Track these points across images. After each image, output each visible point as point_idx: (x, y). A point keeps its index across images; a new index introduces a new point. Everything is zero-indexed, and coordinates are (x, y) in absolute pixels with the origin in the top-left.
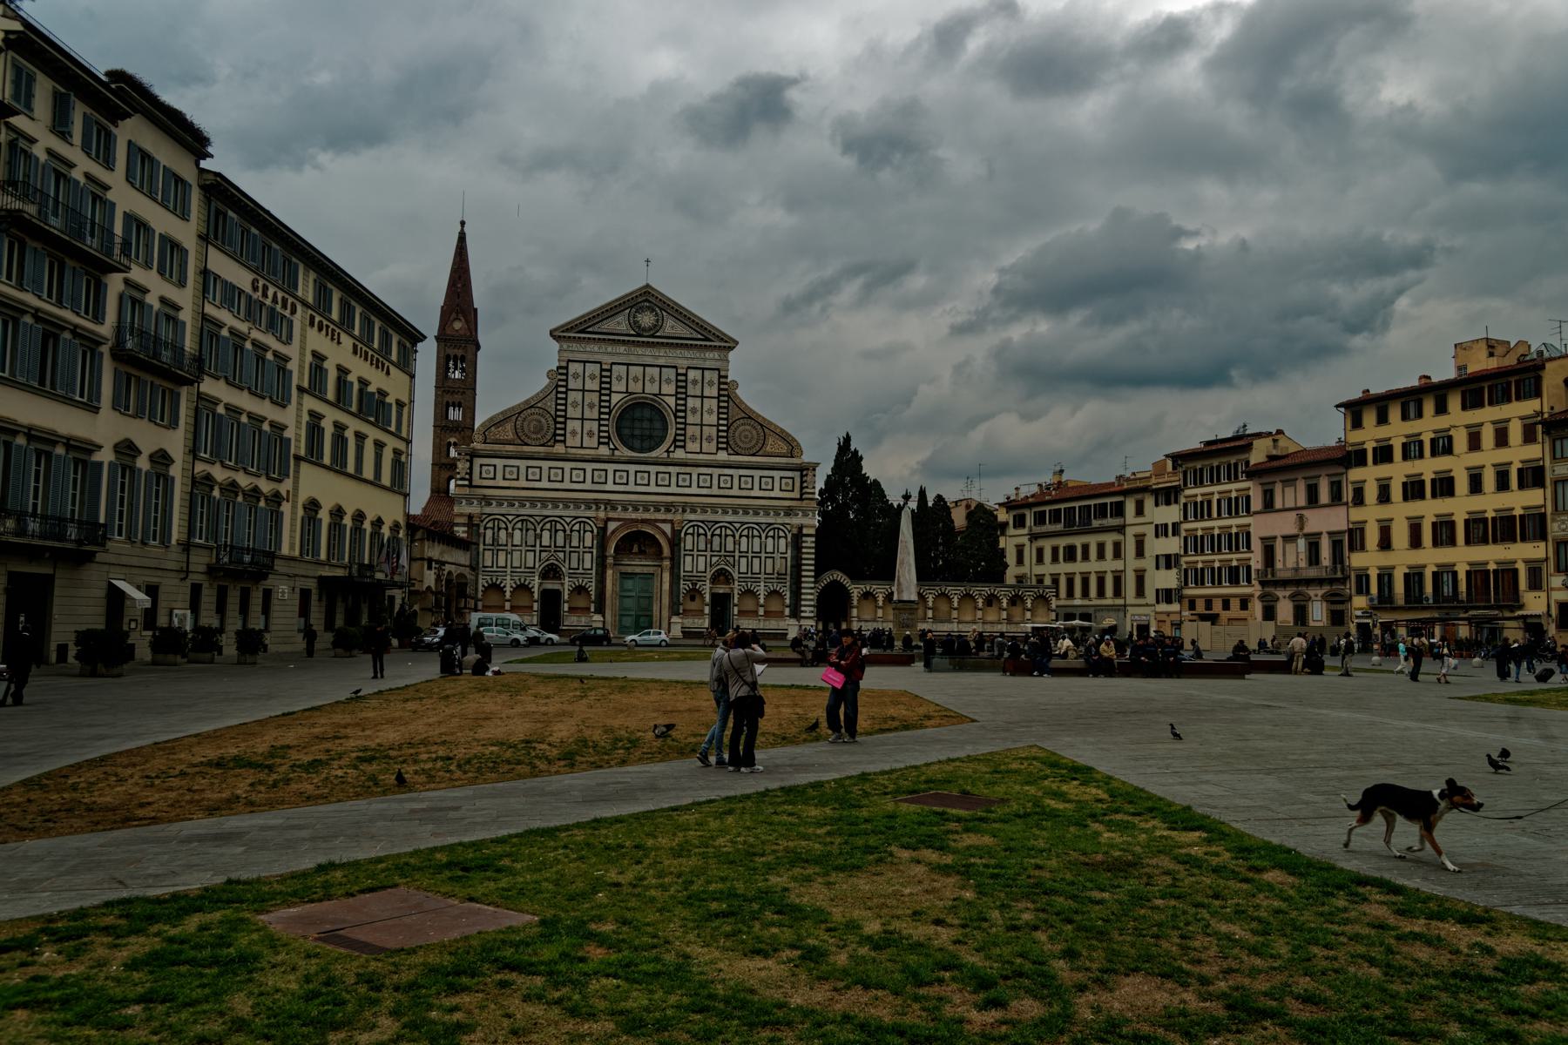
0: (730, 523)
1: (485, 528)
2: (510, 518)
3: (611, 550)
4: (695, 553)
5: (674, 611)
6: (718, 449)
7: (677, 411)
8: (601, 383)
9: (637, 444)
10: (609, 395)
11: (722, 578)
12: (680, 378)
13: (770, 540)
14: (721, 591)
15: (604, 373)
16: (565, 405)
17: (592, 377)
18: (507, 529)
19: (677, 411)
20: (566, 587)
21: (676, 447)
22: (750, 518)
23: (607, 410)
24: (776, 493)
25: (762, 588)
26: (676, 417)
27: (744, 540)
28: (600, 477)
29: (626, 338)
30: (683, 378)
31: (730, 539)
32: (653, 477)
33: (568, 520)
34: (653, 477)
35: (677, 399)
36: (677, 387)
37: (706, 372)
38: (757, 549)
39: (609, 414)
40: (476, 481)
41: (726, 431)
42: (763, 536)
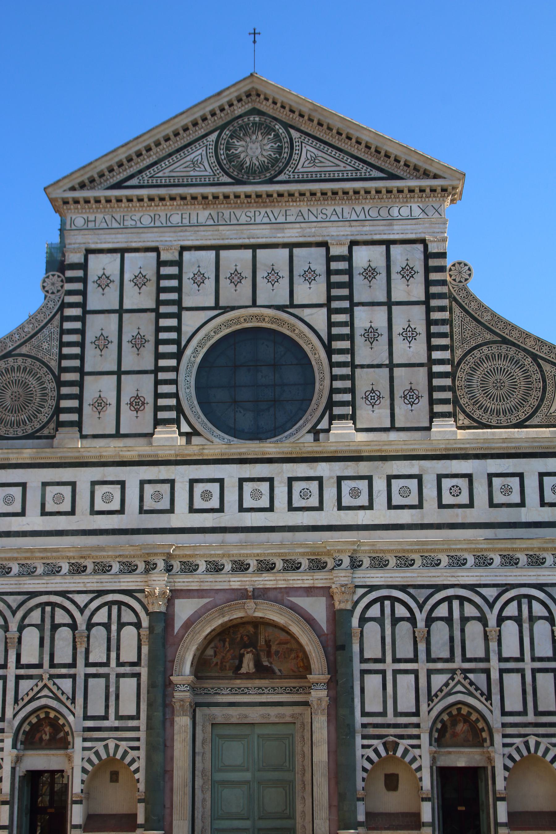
0: (472, 587)
4: (389, 666)
6: (433, 415)
7: (332, 337)
8: (160, 290)
10: (178, 316)
11: (461, 727)
12: (334, 266)
14: (461, 763)
15: (165, 271)
16: (82, 345)
20: (78, 763)
21: (332, 418)
23: (173, 348)
26: (330, 352)
28: (157, 496)
29: (209, 191)
30: (343, 265)
32: (281, 491)
33: (81, 600)
34: (281, 491)
35: (331, 312)
36: (330, 286)
37: (395, 250)
39: (178, 356)
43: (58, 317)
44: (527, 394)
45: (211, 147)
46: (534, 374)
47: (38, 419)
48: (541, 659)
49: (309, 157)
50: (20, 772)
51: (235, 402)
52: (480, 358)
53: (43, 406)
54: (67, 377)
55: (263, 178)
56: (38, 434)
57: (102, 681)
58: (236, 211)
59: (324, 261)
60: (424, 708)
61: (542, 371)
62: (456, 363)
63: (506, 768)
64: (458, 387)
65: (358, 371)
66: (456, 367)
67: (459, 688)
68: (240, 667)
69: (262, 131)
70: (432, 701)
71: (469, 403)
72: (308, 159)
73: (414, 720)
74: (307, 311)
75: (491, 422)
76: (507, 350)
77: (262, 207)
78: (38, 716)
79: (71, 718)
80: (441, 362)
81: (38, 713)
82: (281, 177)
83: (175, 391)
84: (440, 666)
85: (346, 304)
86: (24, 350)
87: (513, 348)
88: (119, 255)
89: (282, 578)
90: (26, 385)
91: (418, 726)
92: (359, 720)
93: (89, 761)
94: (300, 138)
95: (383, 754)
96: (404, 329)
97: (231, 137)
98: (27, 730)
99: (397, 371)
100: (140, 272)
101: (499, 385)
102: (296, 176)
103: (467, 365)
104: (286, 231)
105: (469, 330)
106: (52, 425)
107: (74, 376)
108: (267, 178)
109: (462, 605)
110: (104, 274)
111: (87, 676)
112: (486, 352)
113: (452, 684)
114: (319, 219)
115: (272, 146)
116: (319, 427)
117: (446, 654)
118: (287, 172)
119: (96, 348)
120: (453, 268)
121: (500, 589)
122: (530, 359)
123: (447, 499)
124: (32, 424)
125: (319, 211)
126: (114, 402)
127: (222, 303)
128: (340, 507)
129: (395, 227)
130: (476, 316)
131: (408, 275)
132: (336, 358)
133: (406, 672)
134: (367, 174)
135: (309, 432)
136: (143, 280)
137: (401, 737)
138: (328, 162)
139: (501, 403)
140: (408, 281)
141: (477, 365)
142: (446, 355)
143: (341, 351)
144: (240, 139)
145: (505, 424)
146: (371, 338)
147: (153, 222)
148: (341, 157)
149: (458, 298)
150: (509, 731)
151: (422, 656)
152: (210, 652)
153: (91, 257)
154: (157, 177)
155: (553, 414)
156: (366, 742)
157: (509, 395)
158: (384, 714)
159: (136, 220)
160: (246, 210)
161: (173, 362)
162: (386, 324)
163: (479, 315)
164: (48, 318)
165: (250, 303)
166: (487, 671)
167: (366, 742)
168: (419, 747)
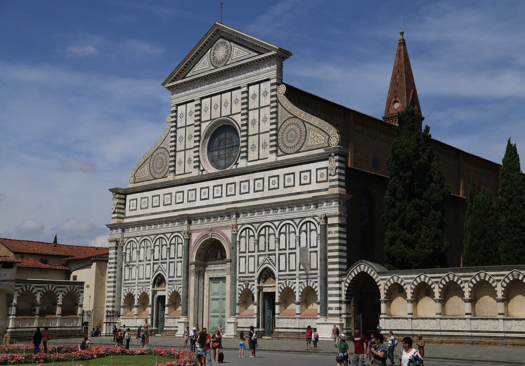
0: (271, 222)
1: (126, 249)
2: (138, 239)
3: (193, 259)
4: (247, 254)
5: (233, 314)
6: (271, 152)
7: (242, 125)
9: (222, 163)
10: (200, 125)
13: (303, 235)
16: (175, 141)
18: (136, 248)
19: (242, 125)
21: (242, 158)
22: (288, 214)
23: (197, 138)
24: (314, 186)
25: (297, 285)
27: (283, 237)
30: (245, 95)
31: (272, 238)
37: (262, 84)
38: (292, 245)
39: (199, 141)
40: (128, 213)
41: (276, 135)
42: (297, 231)
44: (300, 138)
48: (292, 249)
50: (156, 296)
55: (223, 64)
57: (173, 264)
60: (256, 270)
61: (305, 127)
63: (279, 292)
65: (249, 137)
67: (267, 262)
68: (217, 256)
70: (259, 267)
73: (253, 275)
74: (235, 116)
78: (160, 277)
79: (166, 278)
81: (160, 276)
82: (228, 63)
84: (262, 253)
86: (162, 146)
89: (219, 223)
90: (162, 159)
91: (254, 277)
92: (238, 275)
93: (170, 292)
95: (245, 288)
98: (158, 281)
101: (291, 136)
104: (229, 85)
106: (168, 172)
107: (172, 154)
109: (269, 229)
111: (170, 262)
112: (288, 122)
113: (265, 260)
117: (263, 249)
120: (279, 88)
121: (280, 222)
122: (302, 123)
123: (272, 187)
128: (240, 194)
129: (260, 76)
130: (286, 107)
133: (252, 256)
137: (250, 281)
141: (285, 129)
142: (274, 126)
143: (243, 131)
144: (216, 50)
149: (280, 101)
150: (281, 278)
151: (256, 250)
152: (209, 251)
156: (240, 283)
158: (245, 273)
161: (197, 144)
165: (220, 116)
166: (275, 254)
167: (240, 283)
168: (253, 285)
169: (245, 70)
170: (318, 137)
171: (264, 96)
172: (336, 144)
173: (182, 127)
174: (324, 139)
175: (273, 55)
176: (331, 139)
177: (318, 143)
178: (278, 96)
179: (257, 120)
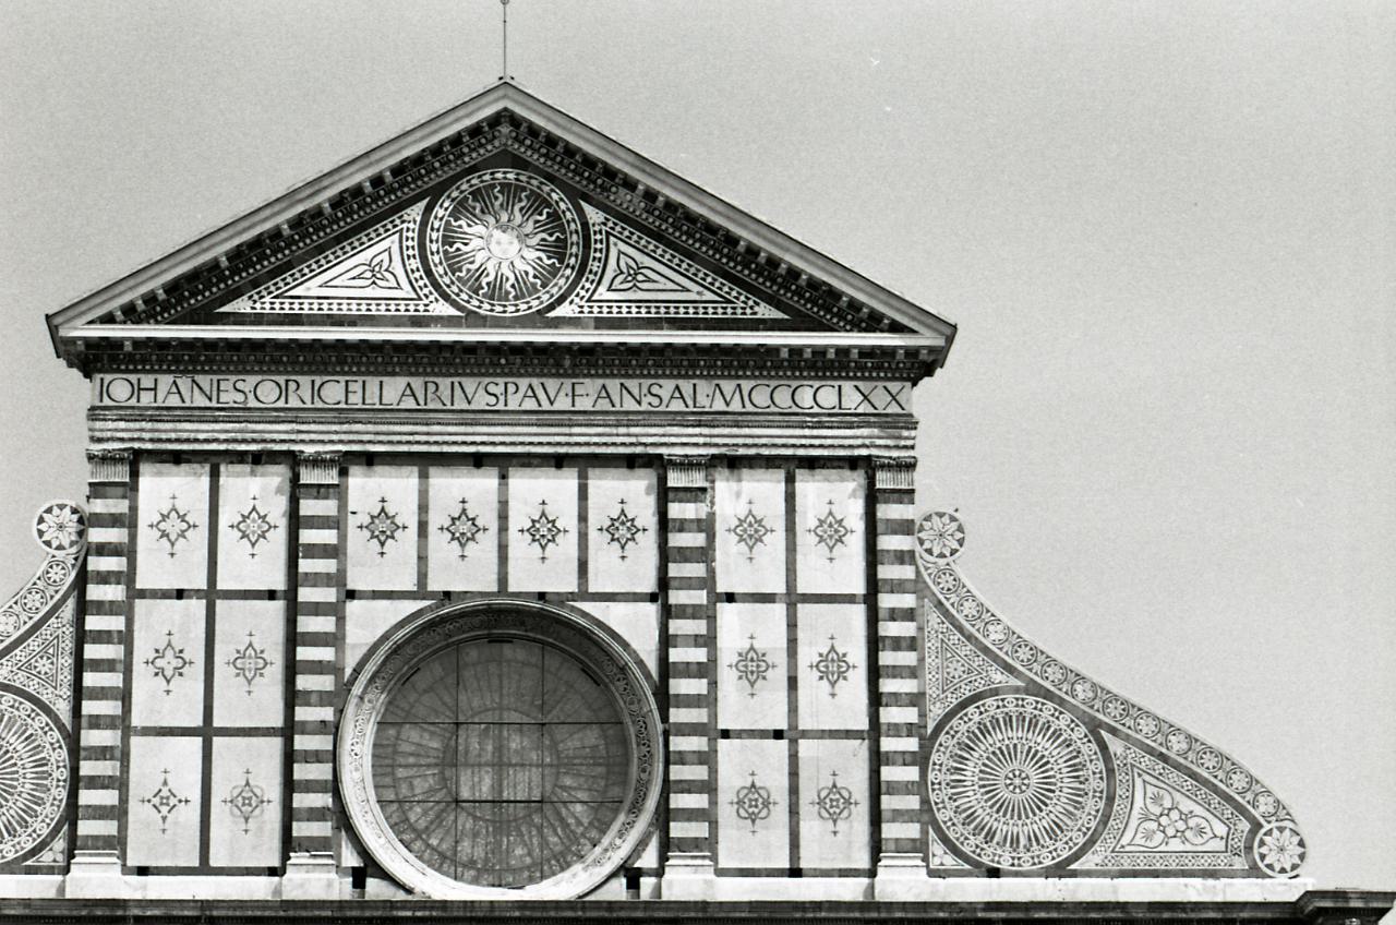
17: (252, 529)
23: (325, 683)
35: (668, 612)
36: (665, 555)
43: (71, 603)
45: (410, 234)
46: (1091, 761)
47: (30, 830)
49: (625, 270)
51: (457, 802)
52: (980, 723)
53: (39, 802)
54: (91, 738)
56: (29, 863)
58: (464, 380)
59: (650, 502)
62: (929, 731)
64: (933, 784)
65: (722, 744)
66: (928, 743)
69: (523, 204)
71: (955, 821)
72: (622, 273)
75: (999, 863)
76: (1035, 708)
77: (521, 376)
80: (896, 730)
82: (564, 310)
83: (330, 777)
85: (700, 597)
87: (1050, 705)
88: (207, 467)
94: (605, 224)
96: (821, 655)
97: (455, 215)
99: (806, 747)
100: (254, 509)
101: (1017, 781)
102: (596, 310)
103: (953, 737)
105: (958, 661)
108: (534, 310)
110: (174, 509)
114: (645, 407)
115: (543, 240)
116: (636, 866)
118: (577, 300)
119: (157, 674)
120: (927, 525)
122: (1083, 729)
124: (17, 840)
125: (645, 391)
126: (195, 796)
127: (435, 585)
131: (831, 537)
132: (678, 715)
134: (748, 311)
135: (613, 875)
136: (259, 527)
138: (663, 280)
139: (1020, 823)
140: (831, 549)
142: (909, 715)
145: (1026, 867)
146: (752, 672)
147: (283, 399)
148: (693, 270)
153: (144, 468)
154: (292, 297)
155: (1128, 849)
157: (1041, 804)
159: (247, 390)
160: (487, 380)
161: (327, 714)
162: (782, 642)
163: (978, 630)
164: (51, 604)
165: (495, 588)
169: (694, 376)
170: (1185, 817)
171: (821, 539)
172: (1294, 867)
173: (180, 594)
174: (1221, 830)
175: (912, 353)
176: (1267, 839)
177: (1188, 847)
178: (920, 562)
179: (781, 659)
